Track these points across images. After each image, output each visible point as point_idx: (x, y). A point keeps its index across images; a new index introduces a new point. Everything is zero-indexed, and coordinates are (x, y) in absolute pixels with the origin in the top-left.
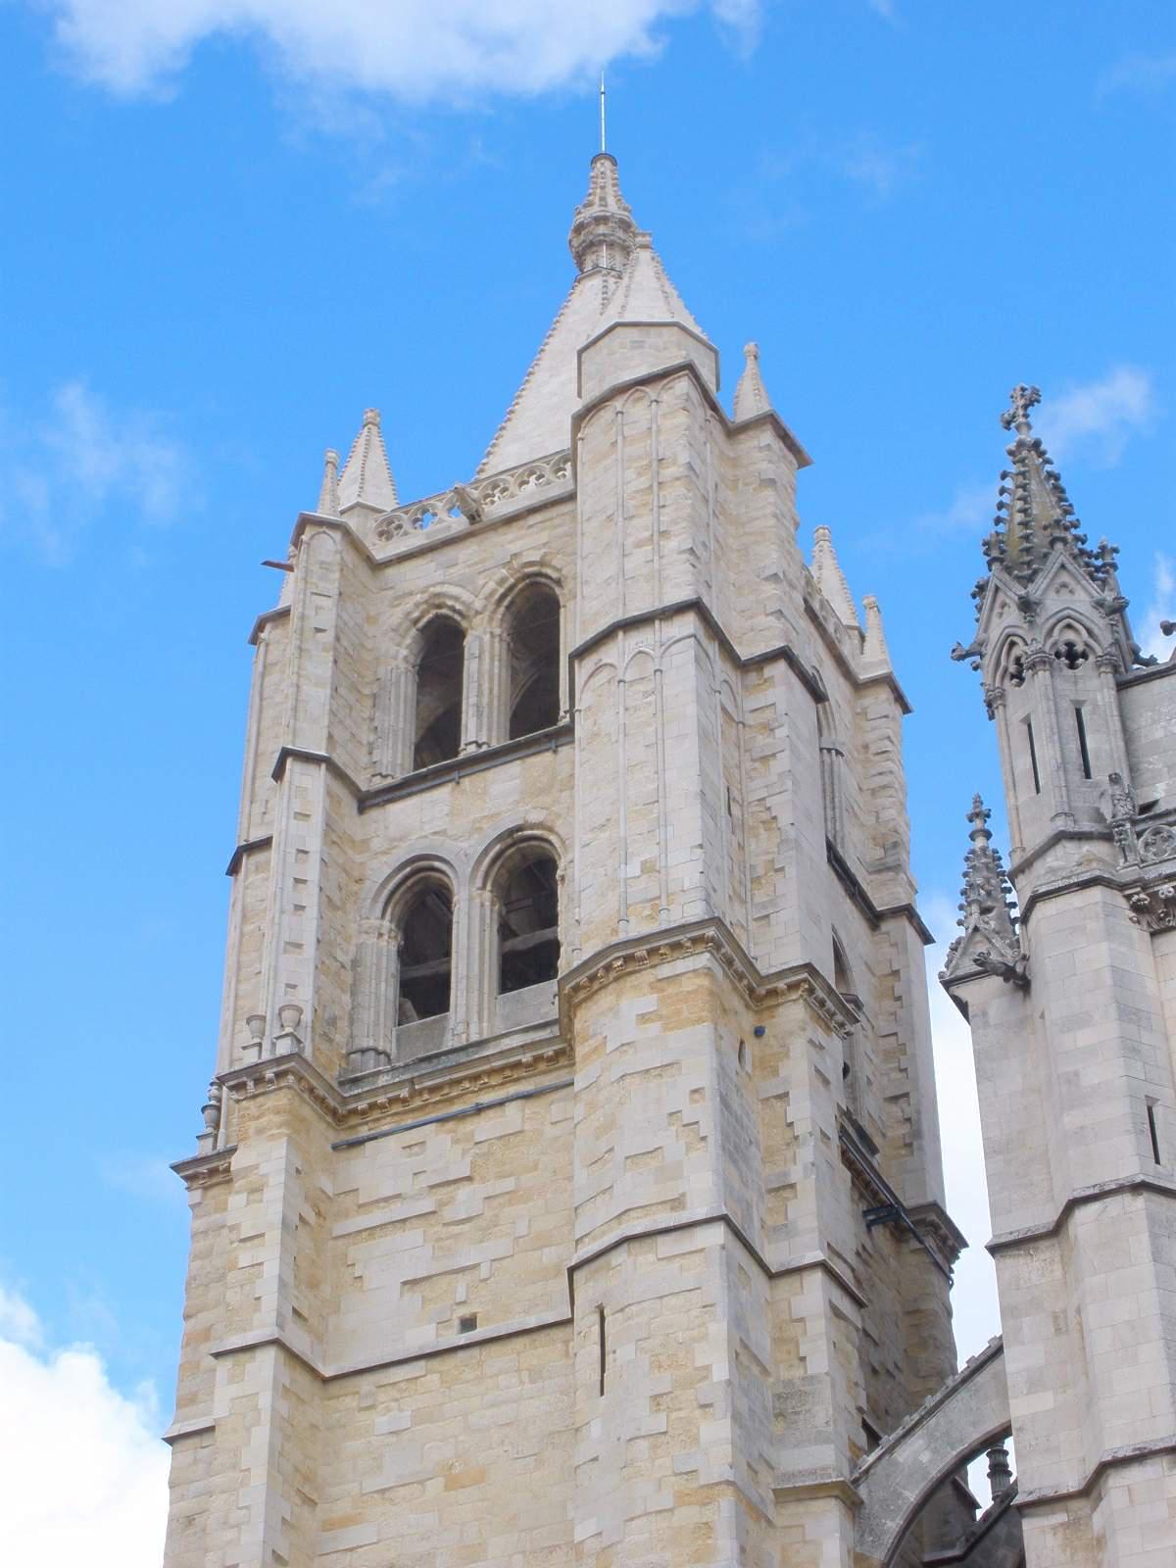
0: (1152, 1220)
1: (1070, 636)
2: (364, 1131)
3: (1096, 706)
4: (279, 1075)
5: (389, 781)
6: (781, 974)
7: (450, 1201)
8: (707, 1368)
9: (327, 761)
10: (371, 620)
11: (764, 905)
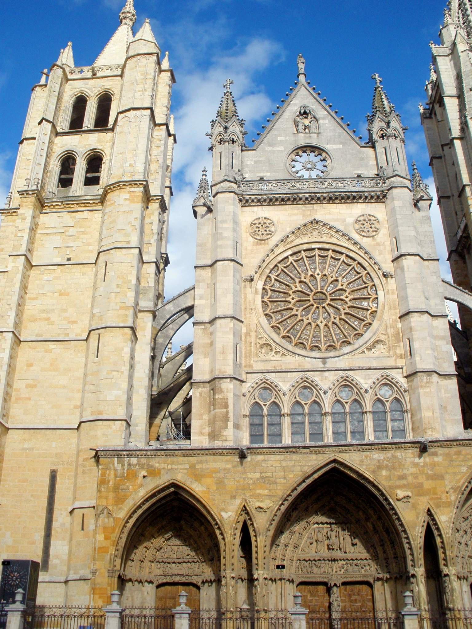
0: (234, 267)
1: (233, 137)
3: (236, 154)
4: (33, 194)
5: (64, 131)
8: (131, 280)
9: (52, 123)
11: (153, 180)
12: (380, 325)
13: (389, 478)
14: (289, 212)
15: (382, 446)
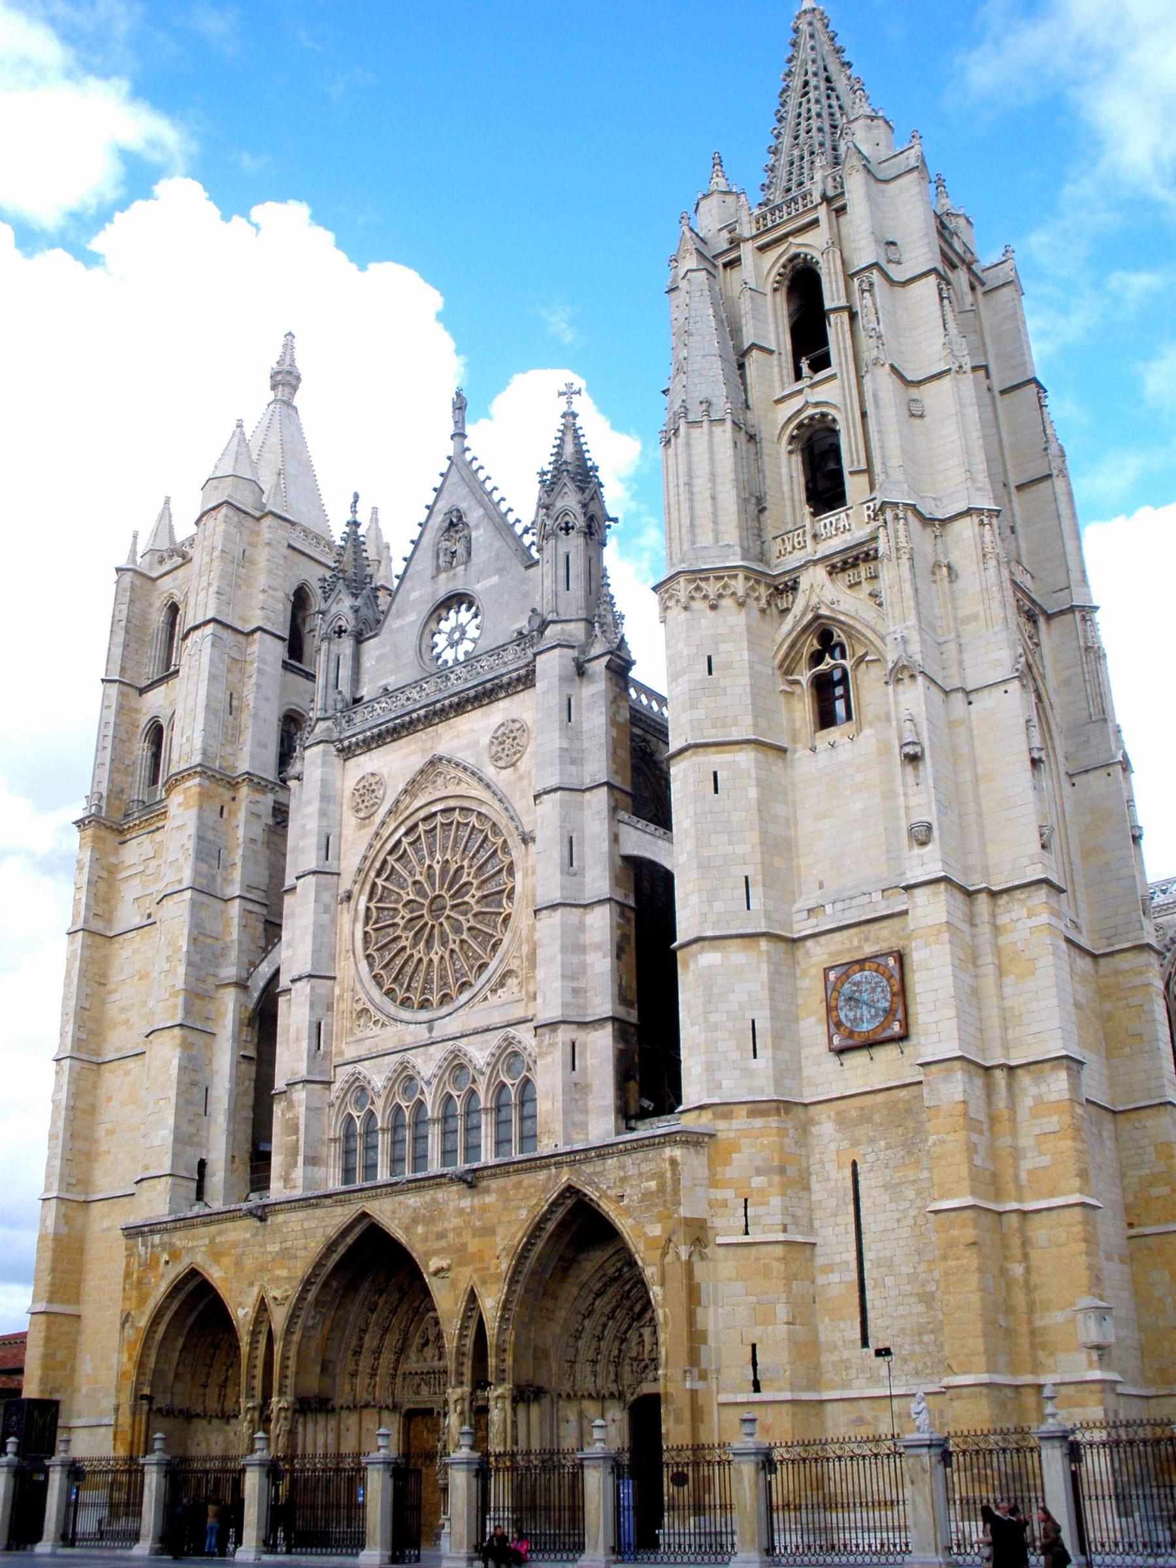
0: (317, 885)
2: (128, 837)
6: (239, 776)
7: (146, 867)
10: (151, 605)
12: (512, 941)
13: (425, 1239)
14: (405, 751)
15: (418, 1185)
